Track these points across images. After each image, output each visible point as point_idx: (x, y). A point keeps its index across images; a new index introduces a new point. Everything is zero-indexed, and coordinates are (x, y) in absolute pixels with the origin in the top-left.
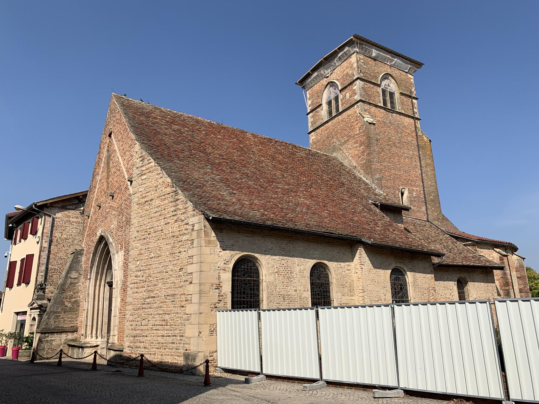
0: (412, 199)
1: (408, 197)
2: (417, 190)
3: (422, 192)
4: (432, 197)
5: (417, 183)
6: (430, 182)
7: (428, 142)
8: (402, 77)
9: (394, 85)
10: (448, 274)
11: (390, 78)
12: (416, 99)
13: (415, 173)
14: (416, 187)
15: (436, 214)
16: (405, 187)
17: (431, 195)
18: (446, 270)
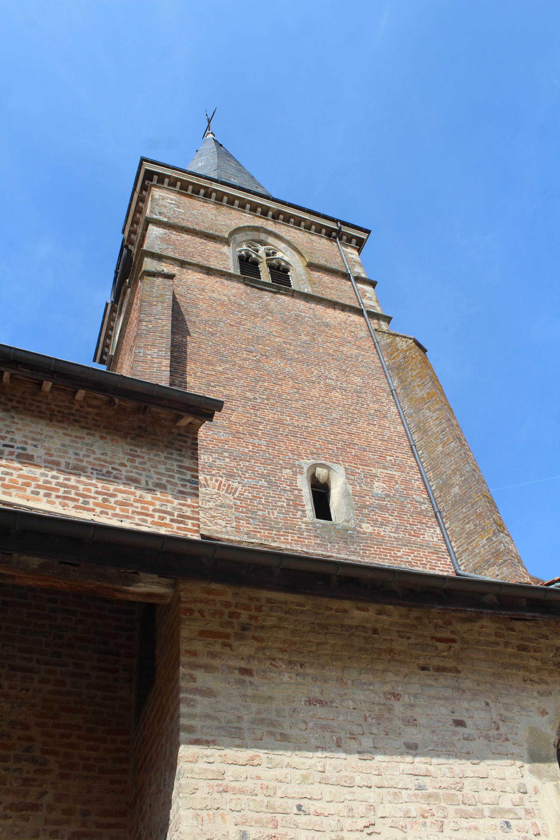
0: (368, 501)
1: (346, 494)
2: (391, 478)
3: (418, 484)
4: (456, 490)
5: (388, 458)
6: (440, 448)
7: (411, 349)
8: (315, 244)
9: (288, 253)
10: (457, 689)
11: (271, 240)
12: (373, 284)
13: (375, 429)
14: (385, 468)
15: (485, 541)
16: (328, 464)
17: (452, 485)
18: (436, 662)
